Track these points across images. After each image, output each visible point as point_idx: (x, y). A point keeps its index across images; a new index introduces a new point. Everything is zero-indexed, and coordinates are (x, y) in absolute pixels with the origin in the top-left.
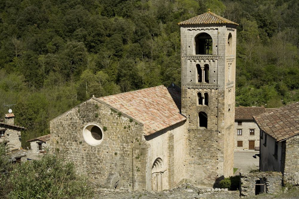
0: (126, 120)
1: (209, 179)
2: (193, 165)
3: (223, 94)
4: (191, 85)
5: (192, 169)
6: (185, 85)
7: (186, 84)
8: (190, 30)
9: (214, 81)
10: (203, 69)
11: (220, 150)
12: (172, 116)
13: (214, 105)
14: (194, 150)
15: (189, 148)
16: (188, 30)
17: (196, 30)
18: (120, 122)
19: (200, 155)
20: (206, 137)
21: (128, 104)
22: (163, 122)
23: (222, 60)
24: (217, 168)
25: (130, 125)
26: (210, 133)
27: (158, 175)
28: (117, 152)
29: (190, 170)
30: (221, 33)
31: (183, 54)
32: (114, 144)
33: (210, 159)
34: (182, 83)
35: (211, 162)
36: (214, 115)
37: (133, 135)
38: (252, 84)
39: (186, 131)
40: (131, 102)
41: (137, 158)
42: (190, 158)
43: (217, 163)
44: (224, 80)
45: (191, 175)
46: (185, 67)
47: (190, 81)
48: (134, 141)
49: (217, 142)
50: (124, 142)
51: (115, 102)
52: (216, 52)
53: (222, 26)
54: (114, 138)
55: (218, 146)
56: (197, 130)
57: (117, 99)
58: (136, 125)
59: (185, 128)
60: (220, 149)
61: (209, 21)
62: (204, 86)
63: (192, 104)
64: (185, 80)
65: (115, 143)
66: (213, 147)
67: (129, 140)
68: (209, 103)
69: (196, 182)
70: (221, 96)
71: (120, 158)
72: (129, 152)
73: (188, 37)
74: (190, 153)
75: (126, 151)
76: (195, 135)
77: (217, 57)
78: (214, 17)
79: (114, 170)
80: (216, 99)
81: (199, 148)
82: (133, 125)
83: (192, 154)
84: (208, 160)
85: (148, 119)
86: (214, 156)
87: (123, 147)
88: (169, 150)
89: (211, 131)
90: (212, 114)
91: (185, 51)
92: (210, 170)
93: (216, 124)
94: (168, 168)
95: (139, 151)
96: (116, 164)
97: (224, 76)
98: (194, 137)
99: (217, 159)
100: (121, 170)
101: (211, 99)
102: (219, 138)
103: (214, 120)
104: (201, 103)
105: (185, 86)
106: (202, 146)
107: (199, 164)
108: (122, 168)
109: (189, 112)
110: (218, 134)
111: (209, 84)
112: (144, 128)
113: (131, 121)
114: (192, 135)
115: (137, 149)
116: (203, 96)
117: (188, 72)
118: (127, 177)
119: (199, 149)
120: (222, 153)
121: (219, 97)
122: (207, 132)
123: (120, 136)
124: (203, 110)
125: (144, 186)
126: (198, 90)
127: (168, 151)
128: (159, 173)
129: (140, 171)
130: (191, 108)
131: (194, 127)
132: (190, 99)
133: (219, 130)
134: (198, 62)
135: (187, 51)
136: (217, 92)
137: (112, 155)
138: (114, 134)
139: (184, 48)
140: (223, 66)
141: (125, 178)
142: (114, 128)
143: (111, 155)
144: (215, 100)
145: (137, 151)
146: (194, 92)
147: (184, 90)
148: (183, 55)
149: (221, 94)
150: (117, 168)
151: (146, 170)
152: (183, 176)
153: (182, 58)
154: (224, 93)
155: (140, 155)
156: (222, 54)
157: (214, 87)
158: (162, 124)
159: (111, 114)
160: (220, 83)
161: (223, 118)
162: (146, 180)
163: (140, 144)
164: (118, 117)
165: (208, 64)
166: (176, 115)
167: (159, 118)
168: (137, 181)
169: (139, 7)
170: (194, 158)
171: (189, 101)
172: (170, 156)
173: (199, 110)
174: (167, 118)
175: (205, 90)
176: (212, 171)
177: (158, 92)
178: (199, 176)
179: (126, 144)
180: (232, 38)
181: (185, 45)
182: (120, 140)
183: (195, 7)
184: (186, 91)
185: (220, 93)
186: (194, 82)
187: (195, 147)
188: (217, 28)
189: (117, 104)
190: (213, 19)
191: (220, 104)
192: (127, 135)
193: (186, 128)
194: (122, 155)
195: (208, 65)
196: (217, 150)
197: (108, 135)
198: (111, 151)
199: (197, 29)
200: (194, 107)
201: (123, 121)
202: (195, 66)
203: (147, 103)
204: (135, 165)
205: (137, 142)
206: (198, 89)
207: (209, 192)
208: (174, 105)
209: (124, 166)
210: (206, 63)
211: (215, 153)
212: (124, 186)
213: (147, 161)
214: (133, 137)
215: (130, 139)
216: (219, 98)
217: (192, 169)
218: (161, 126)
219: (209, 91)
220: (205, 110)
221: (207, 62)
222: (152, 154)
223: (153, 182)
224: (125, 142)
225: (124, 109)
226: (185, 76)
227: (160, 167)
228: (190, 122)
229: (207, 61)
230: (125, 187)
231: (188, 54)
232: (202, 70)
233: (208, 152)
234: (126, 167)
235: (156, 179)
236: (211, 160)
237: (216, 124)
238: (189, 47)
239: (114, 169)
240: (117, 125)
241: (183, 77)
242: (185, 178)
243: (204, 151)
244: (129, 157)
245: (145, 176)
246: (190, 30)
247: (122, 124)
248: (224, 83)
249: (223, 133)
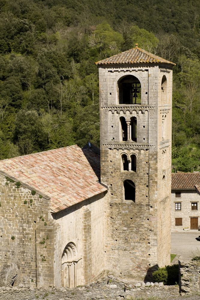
0: (27, 193)
1: (139, 270)
2: (117, 252)
3: (155, 157)
4: (113, 144)
5: (116, 256)
6: (106, 145)
7: (106, 144)
8: (111, 71)
9: (144, 139)
10: (128, 123)
11: (153, 231)
12: (88, 186)
13: (143, 171)
14: (118, 231)
15: (112, 228)
16: (109, 71)
17: (119, 72)
18: (18, 196)
19: (127, 238)
20: (133, 214)
21: (29, 170)
22: (77, 194)
23: (153, 111)
24: (149, 255)
25: (32, 198)
26: (139, 207)
27: (70, 265)
28: (14, 235)
29: (113, 258)
30: (152, 75)
31: (102, 103)
32: (10, 225)
33: (139, 243)
34: (102, 142)
35: (140, 246)
36: (145, 185)
37: (36, 212)
38: (194, 142)
39: (107, 205)
40: (34, 168)
41: (42, 243)
42: (113, 242)
43: (148, 248)
44: (157, 138)
45: (115, 264)
47: (112, 139)
48: (37, 220)
49: (148, 219)
50: (24, 222)
51: (11, 168)
52: (146, 101)
53: (154, 67)
54: (11, 217)
55: (150, 225)
56: (122, 204)
57: (14, 164)
58: (40, 199)
59: (106, 202)
60: (152, 229)
61: (136, 60)
62: (130, 146)
63: (115, 169)
64: (105, 138)
65: (12, 224)
67: (30, 219)
68: (137, 169)
69: (121, 275)
70: (153, 158)
71: (19, 244)
72: (31, 236)
73: (109, 80)
74: (112, 235)
75: (27, 234)
76: (119, 210)
77: (147, 108)
78: (142, 55)
79: (10, 260)
80: (147, 163)
81: (124, 228)
82: (36, 199)
83: (115, 236)
84: (136, 244)
85: (57, 190)
86: (144, 239)
87: (22, 229)
88: (85, 231)
89: (140, 205)
90: (141, 182)
91: (105, 99)
92: (140, 258)
93: (147, 196)
94: (83, 255)
95: (45, 233)
96: (13, 252)
97: (157, 132)
98: (118, 214)
99: (149, 243)
100: (20, 260)
101: (139, 162)
102: (151, 214)
103: (145, 191)
104: (126, 168)
105: (105, 146)
106: (128, 226)
107: (125, 250)
108: (22, 258)
109: (111, 181)
110: (149, 209)
111: (137, 144)
112: (51, 202)
113: (34, 193)
114: (115, 211)
115: (42, 230)
116: (129, 158)
117: (109, 127)
118: (29, 269)
119: (124, 229)
120: (155, 234)
121: (150, 160)
122: (135, 207)
123: (19, 214)
124: (129, 178)
125: (51, 281)
126: (122, 151)
127: (84, 233)
128: (71, 263)
129: (45, 260)
130: (113, 174)
131: (118, 201)
132: (112, 164)
133: (150, 204)
134: (122, 114)
135: (107, 99)
136: (147, 154)
137: (7, 240)
138: (10, 211)
139: (104, 96)
140: (155, 120)
141: (26, 271)
142: (10, 204)
143: (6, 239)
144: (144, 164)
145: (42, 234)
146: (117, 153)
147: (104, 151)
148: (103, 104)
149: (153, 157)
150: (14, 257)
151: (55, 260)
152: (103, 266)
153: (101, 109)
154: (157, 155)
155: (46, 239)
156: (154, 103)
157: (144, 146)
158: (75, 197)
159: (7, 184)
160: (151, 142)
161: (156, 187)
162: (54, 273)
163: (46, 224)
164: (16, 189)
165: (136, 116)
166: (94, 184)
167: (70, 189)
168: (42, 274)
169: (44, 41)
170: (118, 242)
171: (111, 166)
172: (86, 240)
173: (124, 177)
174: (82, 188)
175: (132, 151)
176: (143, 259)
177: (69, 154)
178: (125, 266)
179: (27, 224)
180: (166, 82)
181: (105, 91)
182: (19, 219)
183: (118, 41)
184: (106, 152)
185: (151, 155)
186: (118, 141)
187: (119, 226)
188: (146, 68)
189: (15, 170)
190: (142, 56)
191: (152, 169)
192: (27, 213)
193: (108, 202)
194: (22, 240)
195: (136, 118)
196: (149, 230)
197: (1, 213)
198: (7, 235)
199: (121, 71)
200: (118, 173)
201: (23, 194)
202: (119, 120)
203: (54, 169)
204: (39, 252)
205: (42, 222)
206: (123, 150)
207: (138, 287)
208: (91, 172)
209: (25, 254)
211: (146, 234)
212: (24, 282)
213: (55, 247)
214: (36, 215)
215: (32, 217)
216: (150, 162)
217: (116, 256)
218: (74, 199)
219: (136, 152)
220: (131, 177)
221: (134, 114)
222: (62, 237)
223: (64, 275)
224: (26, 222)
225: (24, 178)
226: (105, 133)
227: (73, 254)
228: (112, 194)
229: (134, 112)
230: (25, 283)
231: (109, 103)
232: (127, 124)
233: (137, 234)
234: (27, 256)
235: (67, 271)
236: (142, 244)
237: (147, 196)
238: (111, 94)
239: (10, 258)
240: (15, 199)
241: (103, 133)
242: (106, 268)
243: (132, 231)
244: (31, 243)
245: (53, 267)
246: (111, 71)
247: (22, 198)
248: (157, 142)
249: (156, 208)
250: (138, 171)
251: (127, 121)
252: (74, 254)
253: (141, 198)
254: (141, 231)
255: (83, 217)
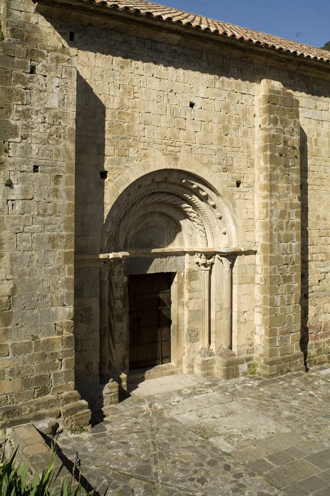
127: (262, 163)
252: (220, 229)
255: (260, 109)
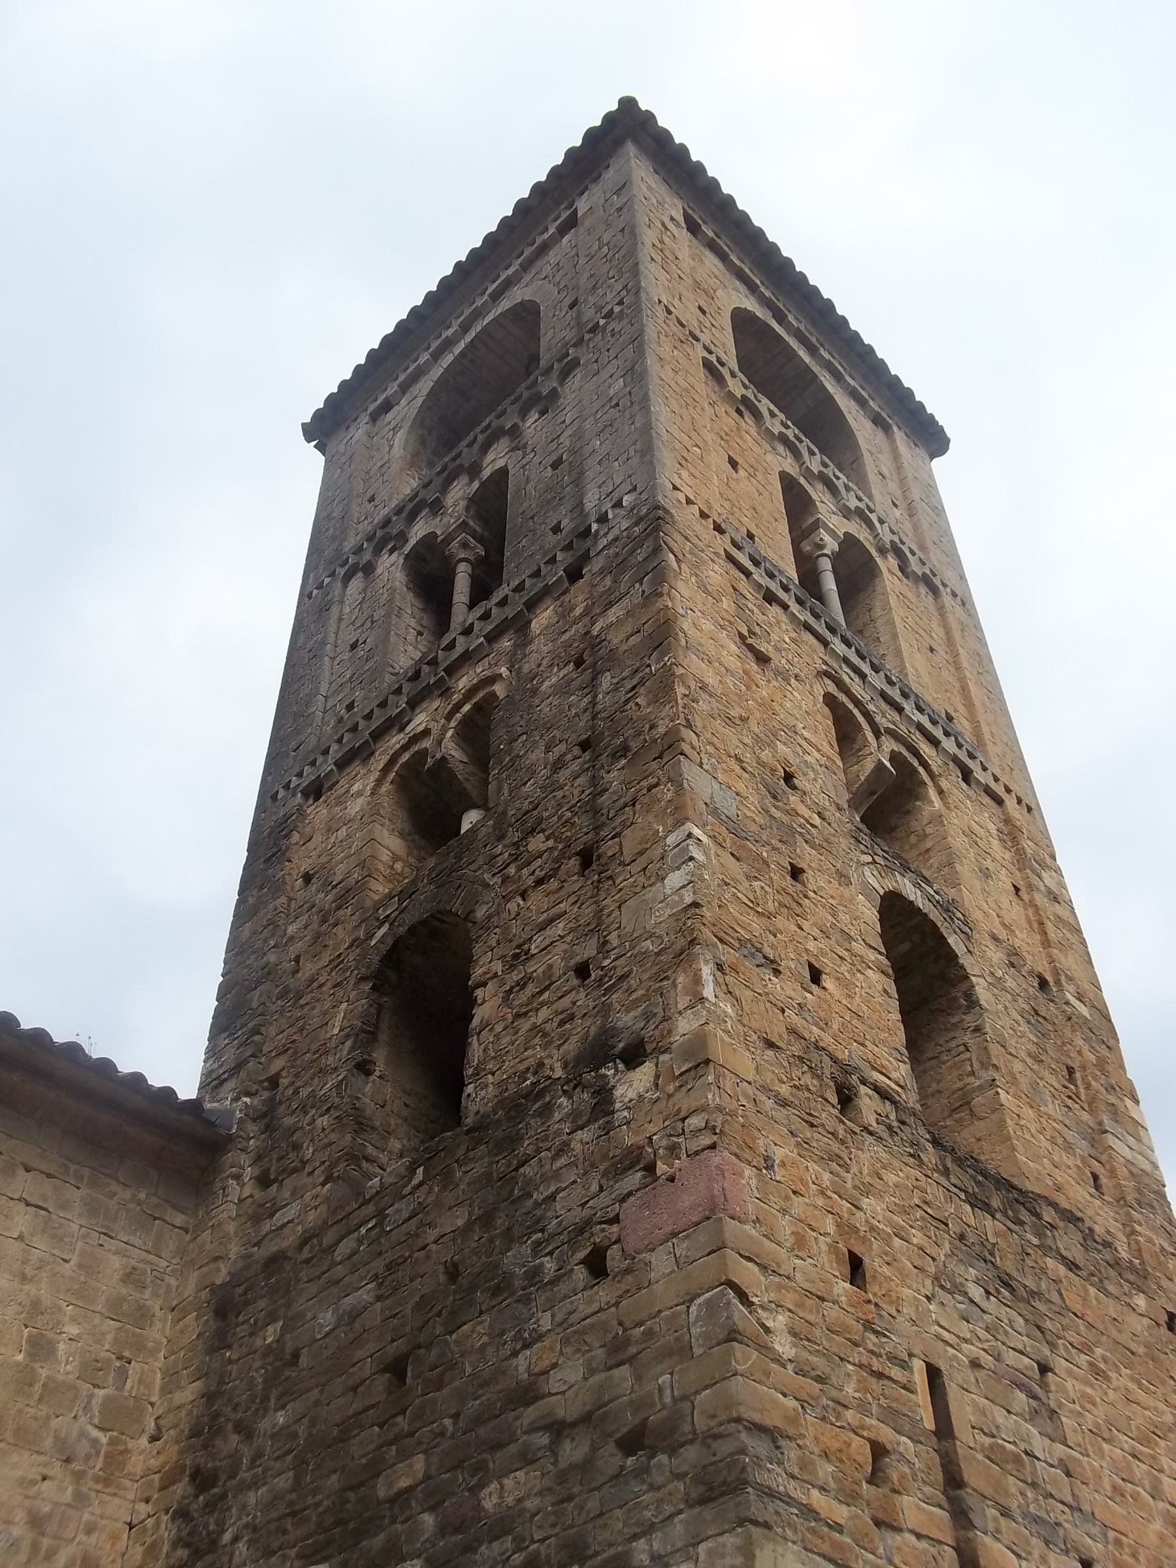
8: (387, 407)
9: (556, 529)
46: (309, 646)
55: (619, 1352)
66: (531, 1414)
93: (582, 971)
103: (560, 928)
144: (564, 689)
210: (486, 473)
250: (500, 789)
251: (448, 540)
253: (525, 1025)
254: (502, 1525)
